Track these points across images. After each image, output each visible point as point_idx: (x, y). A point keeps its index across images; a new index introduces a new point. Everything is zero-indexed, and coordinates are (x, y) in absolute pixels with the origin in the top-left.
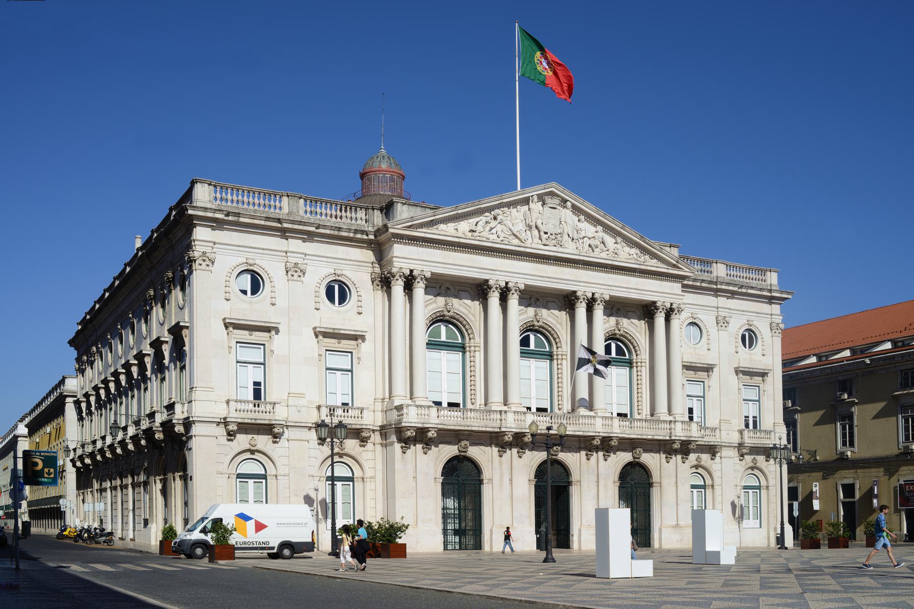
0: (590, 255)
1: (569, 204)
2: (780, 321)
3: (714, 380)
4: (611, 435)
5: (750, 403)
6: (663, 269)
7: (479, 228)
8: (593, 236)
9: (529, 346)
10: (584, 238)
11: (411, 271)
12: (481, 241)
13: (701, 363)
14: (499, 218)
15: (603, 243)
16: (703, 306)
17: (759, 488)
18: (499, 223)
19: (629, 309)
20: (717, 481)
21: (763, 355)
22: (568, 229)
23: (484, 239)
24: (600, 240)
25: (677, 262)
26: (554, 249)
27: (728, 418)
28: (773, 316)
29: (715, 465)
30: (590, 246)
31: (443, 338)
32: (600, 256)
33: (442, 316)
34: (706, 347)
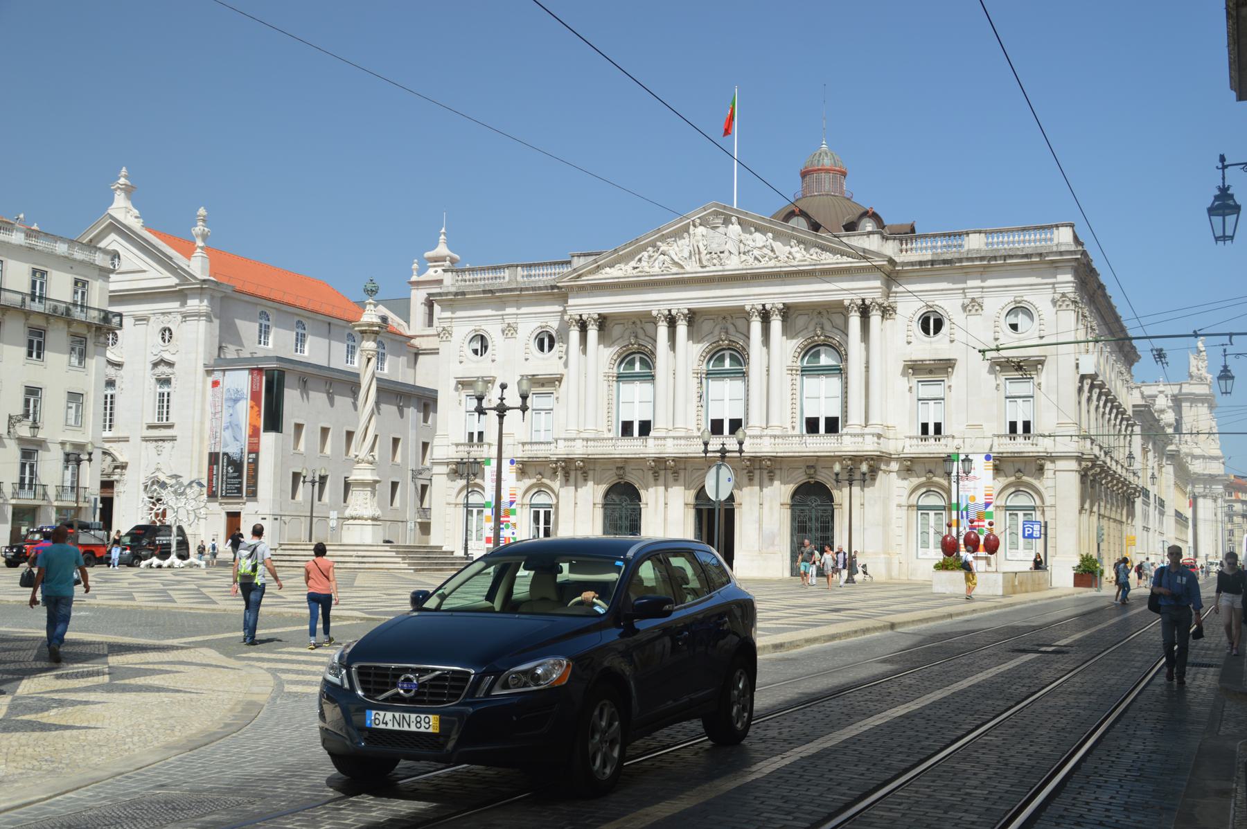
0: (756, 266)
1: (734, 219)
2: (1072, 289)
3: (957, 378)
5: (1020, 401)
6: (845, 262)
7: (644, 263)
14: (661, 249)
15: (773, 250)
16: (942, 290)
18: (661, 254)
19: (834, 310)
22: (730, 246)
23: (643, 274)
24: (769, 247)
25: (864, 252)
30: (756, 258)
32: (767, 265)
34: (947, 339)
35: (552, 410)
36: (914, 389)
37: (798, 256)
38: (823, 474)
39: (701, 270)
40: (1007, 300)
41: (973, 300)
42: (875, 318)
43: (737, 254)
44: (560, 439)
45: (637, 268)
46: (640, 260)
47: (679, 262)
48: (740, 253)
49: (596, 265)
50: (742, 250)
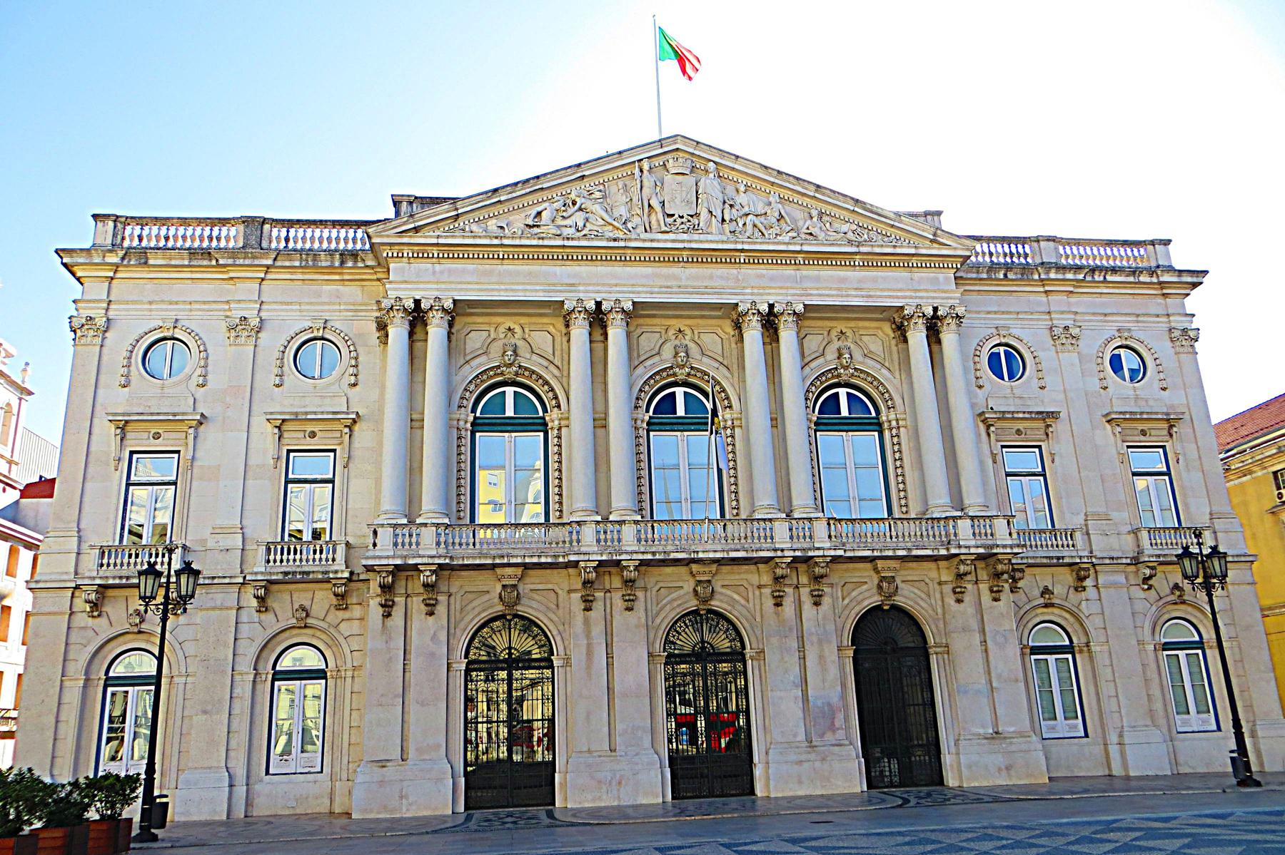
3: (1061, 444)
4: (811, 554)
8: (763, 212)
9: (675, 412)
10: (747, 215)
11: (417, 302)
12: (543, 238)
13: (1024, 412)
17: (1200, 645)
18: (580, 209)
20: (1096, 637)
21: (1164, 389)
24: (777, 214)
25: (935, 235)
26: (685, 237)
27: (1102, 510)
28: (1171, 318)
29: (1088, 604)
31: (510, 412)
33: (502, 374)
34: (1035, 384)
35: (332, 481)
36: (999, 458)
37: (821, 236)
38: (906, 593)
39: (660, 236)
40: (1110, 330)
41: (1066, 328)
42: (949, 337)
43: (720, 220)
44: (382, 525)
45: (534, 226)
46: (539, 214)
47: (615, 223)
48: (723, 220)
49: (454, 213)
50: (727, 218)
